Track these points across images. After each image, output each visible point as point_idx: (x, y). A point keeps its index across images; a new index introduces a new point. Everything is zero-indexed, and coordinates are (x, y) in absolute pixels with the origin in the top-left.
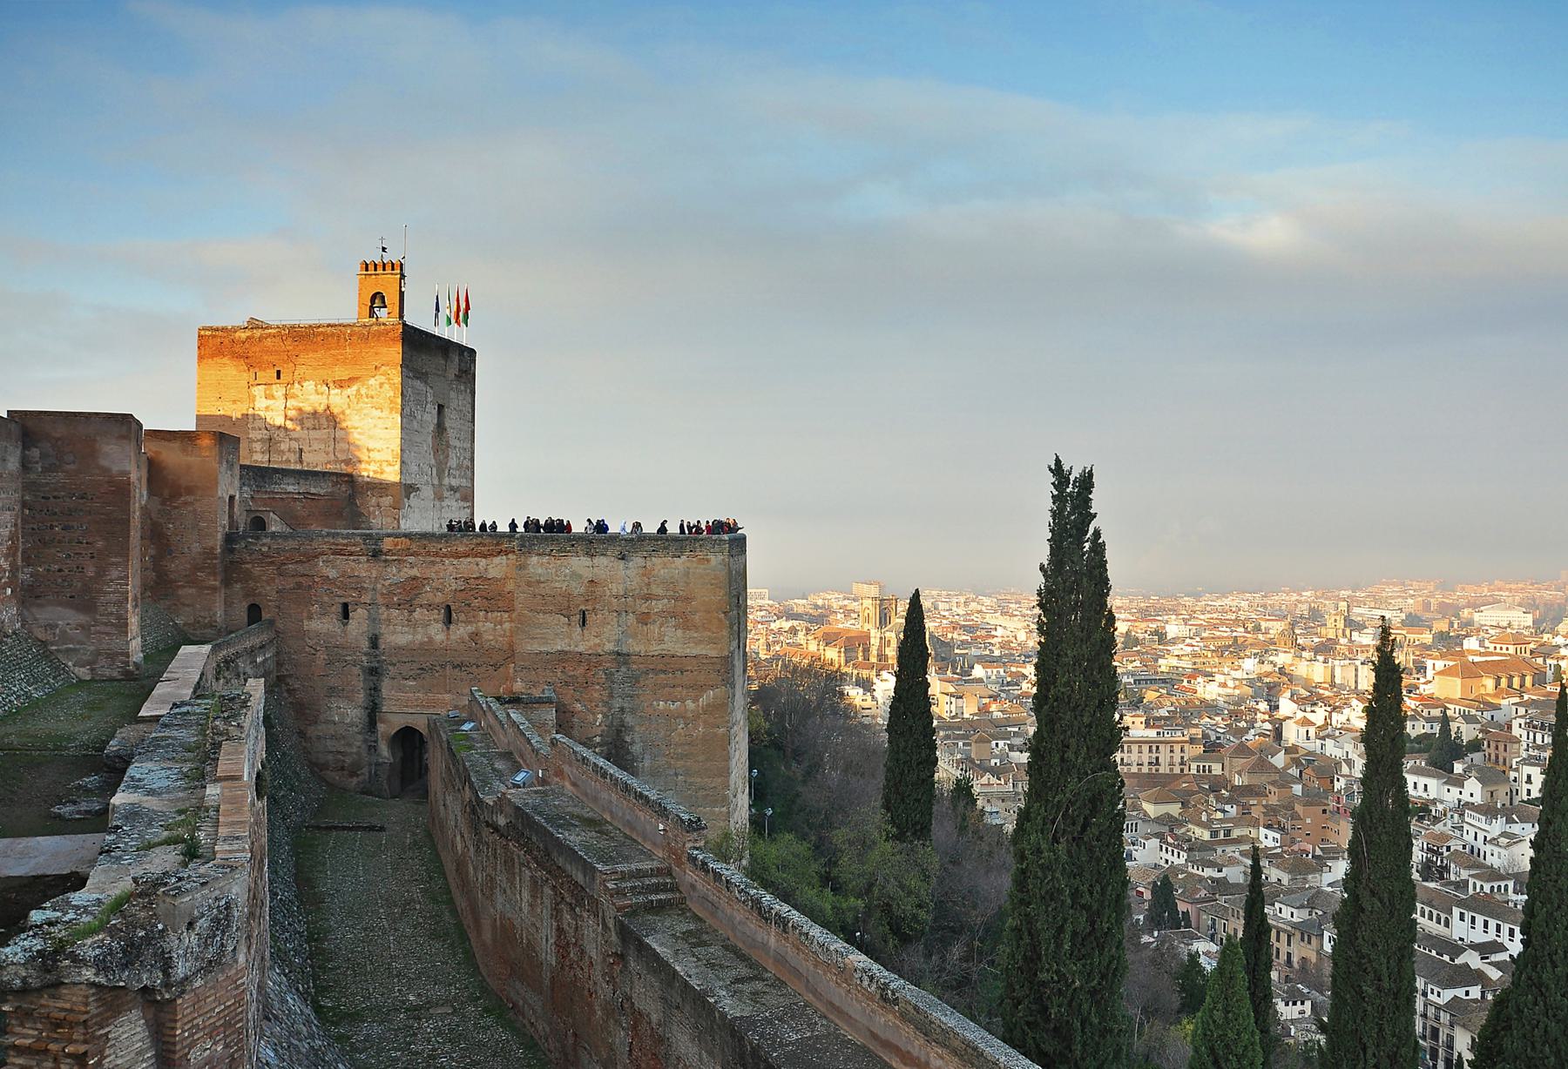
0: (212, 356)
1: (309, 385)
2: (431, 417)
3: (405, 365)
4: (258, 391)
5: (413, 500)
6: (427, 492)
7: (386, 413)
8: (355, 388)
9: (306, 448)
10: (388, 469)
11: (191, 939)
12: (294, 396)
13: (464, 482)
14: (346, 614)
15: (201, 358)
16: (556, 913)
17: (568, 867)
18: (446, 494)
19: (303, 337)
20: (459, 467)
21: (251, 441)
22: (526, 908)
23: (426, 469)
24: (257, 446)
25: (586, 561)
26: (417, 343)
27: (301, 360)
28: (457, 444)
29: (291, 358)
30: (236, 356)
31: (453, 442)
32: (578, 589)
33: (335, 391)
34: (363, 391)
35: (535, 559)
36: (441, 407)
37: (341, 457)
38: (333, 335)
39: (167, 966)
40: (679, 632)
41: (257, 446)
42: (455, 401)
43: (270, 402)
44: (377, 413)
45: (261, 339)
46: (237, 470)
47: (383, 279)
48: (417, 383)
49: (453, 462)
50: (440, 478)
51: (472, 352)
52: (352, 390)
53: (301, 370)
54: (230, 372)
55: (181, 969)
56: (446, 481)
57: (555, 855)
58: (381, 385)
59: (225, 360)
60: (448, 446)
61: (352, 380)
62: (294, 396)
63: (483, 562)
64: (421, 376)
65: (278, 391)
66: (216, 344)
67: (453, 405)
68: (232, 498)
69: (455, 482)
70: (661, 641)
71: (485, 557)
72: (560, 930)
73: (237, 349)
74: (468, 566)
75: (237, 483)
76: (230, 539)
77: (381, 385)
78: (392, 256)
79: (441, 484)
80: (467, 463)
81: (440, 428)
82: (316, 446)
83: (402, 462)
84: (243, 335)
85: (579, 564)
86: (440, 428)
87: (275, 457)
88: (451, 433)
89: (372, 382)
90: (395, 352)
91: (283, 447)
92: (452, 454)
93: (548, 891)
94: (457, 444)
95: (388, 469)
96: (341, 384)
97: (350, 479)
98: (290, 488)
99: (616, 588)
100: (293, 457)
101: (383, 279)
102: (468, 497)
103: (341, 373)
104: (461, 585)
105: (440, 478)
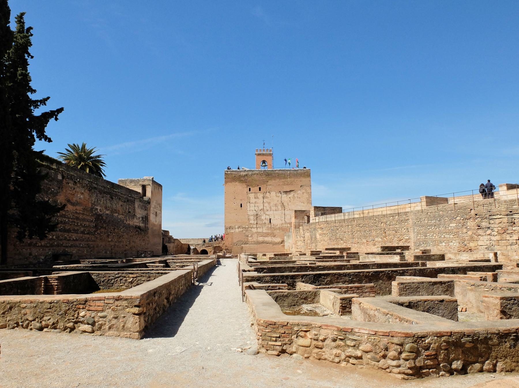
0: (231, 182)
1: (273, 194)
4: (252, 196)
7: (306, 204)
8: (292, 194)
12: (267, 198)
15: (226, 182)
21: (249, 216)
24: (252, 218)
27: (268, 183)
29: (265, 182)
30: (241, 181)
33: (285, 195)
34: (296, 195)
37: (288, 221)
38: (282, 174)
41: (252, 218)
43: (256, 200)
44: (302, 204)
45: (252, 175)
52: (291, 195)
54: (240, 188)
58: (303, 193)
61: (291, 191)
62: (267, 198)
65: (260, 195)
73: (242, 179)
77: (303, 193)
82: (277, 217)
89: (299, 192)
91: (263, 217)
96: (286, 192)
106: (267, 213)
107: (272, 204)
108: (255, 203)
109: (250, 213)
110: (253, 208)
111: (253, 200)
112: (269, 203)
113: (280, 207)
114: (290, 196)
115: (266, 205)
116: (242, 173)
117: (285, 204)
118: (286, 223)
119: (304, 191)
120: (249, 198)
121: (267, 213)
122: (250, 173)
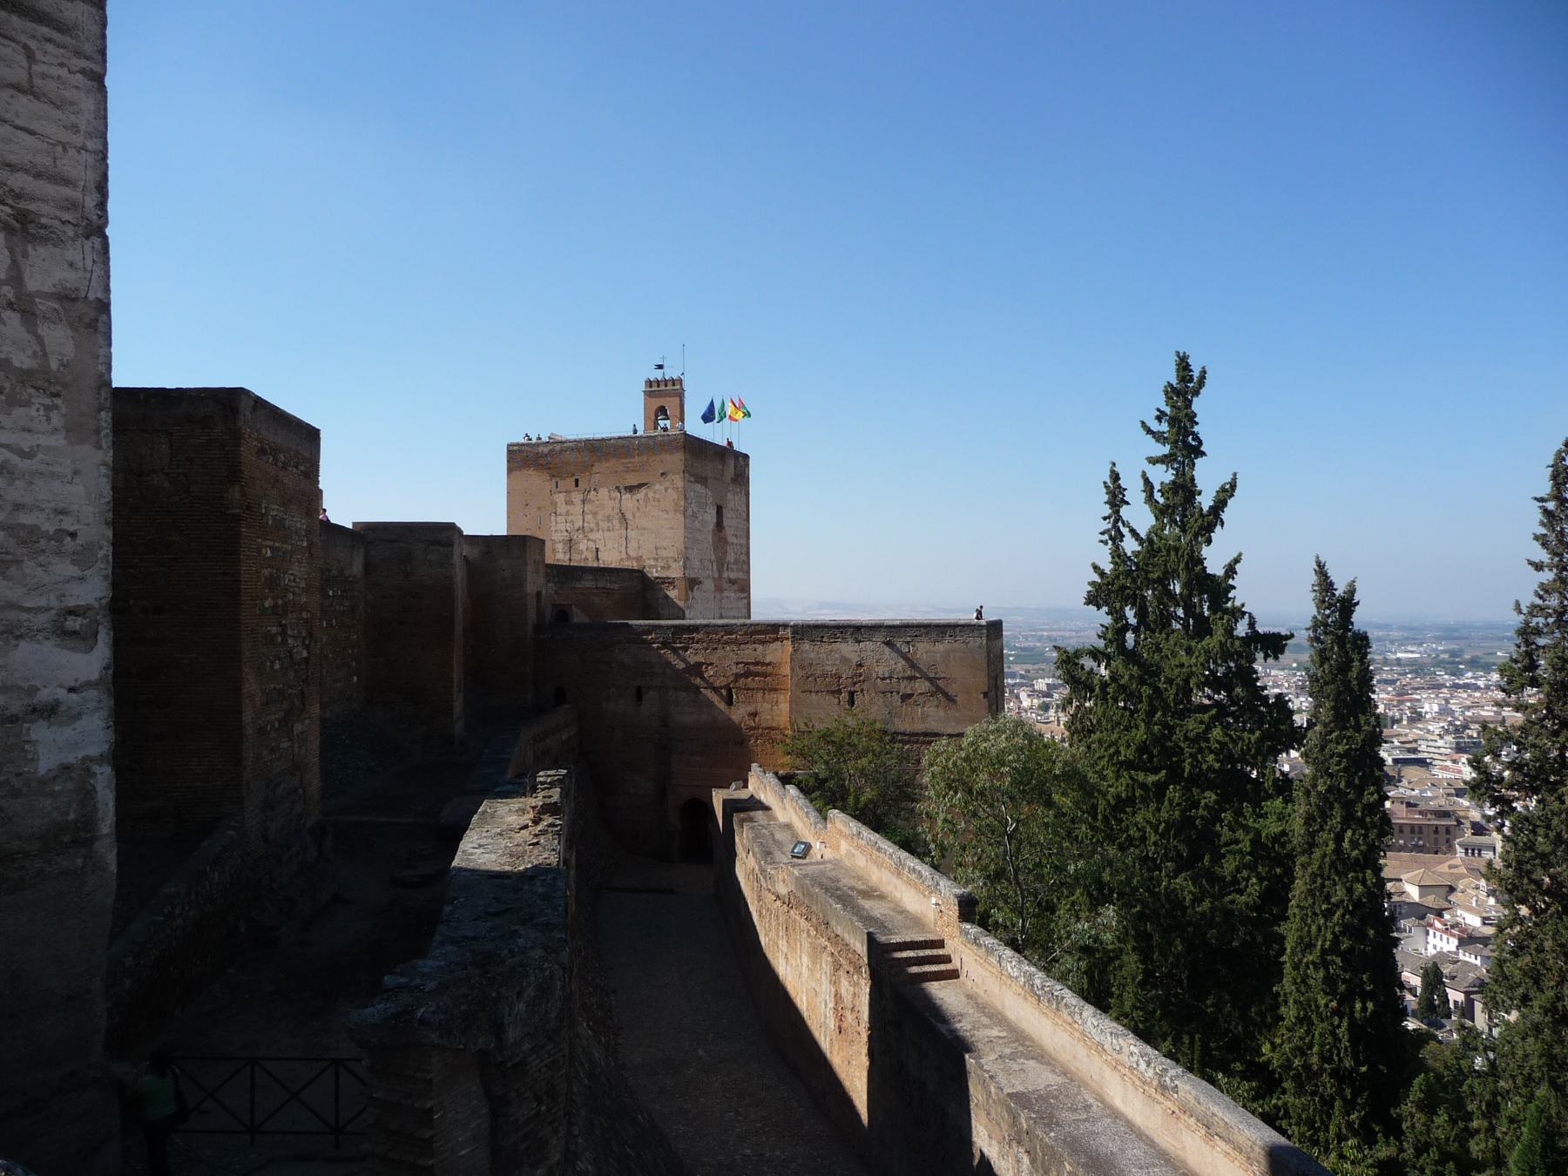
1: (603, 492)
2: (710, 517)
3: (687, 470)
4: (560, 498)
5: (697, 593)
6: (709, 585)
8: (643, 491)
9: (602, 549)
10: (674, 565)
11: (522, 1006)
12: (591, 501)
13: (741, 575)
14: (639, 695)
15: (510, 471)
16: (836, 983)
17: (846, 936)
18: (726, 586)
19: (597, 450)
20: (736, 562)
21: (554, 542)
22: (805, 972)
23: (707, 563)
24: (560, 547)
25: (856, 647)
26: (697, 449)
27: (595, 469)
28: (734, 540)
29: (588, 467)
31: (731, 539)
32: (846, 673)
33: (626, 496)
34: (651, 495)
35: (806, 646)
36: (719, 510)
37: (633, 554)
39: (498, 1029)
40: (941, 713)
41: (560, 547)
42: (732, 501)
46: (541, 570)
47: (664, 395)
48: (699, 488)
49: (731, 557)
50: (720, 573)
51: (746, 457)
53: (596, 478)
54: (536, 480)
55: (512, 1034)
56: (725, 575)
57: (833, 923)
59: (531, 472)
60: (726, 542)
61: (641, 486)
62: (591, 501)
63: (760, 648)
64: (702, 480)
65: (577, 497)
66: (524, 458)
67: (731, 505)
68: (539, 594)
69: (733, 576)
70: (924, 718)
71: (762, 642)
72: (838, 997)
73: (542, 461)
74: (750, 653)
75: (541, 580)
76: (539, 628)
78: (670, 373)
79: (720, 578)
80: (743, 558)
81: (719, 525)
83: (687, 559)
84: (546, 450)
85: (848, 649)
86: (719, 525)
87: (575, 557)
88: (729, 532)
89: (657, 487)
90: (677, 460)
91: (582, 547)
92: (730, 549)
93: (826, 958)
94: (734, 540)
95: (674, 565)
96: (631, 489)
97: (639, 576)
98: (588, 584)
99: (882, 670)
100: (591, 556)
101: (664, 395)
102: (744, 587)
103: (632, 480)
104: (740, 669)
105: (720, 573)
106: (591, 536)
107: (600, 517)
108: (567, 513)
109: (557, 537)
110: (562, 526)
111: (562, 508)
112: (595, 514)
113: (616, 522)
114: (639, 496)
115: (589, 517)
116: (540, 449)
117: (629, 516)
118: (629, 557)
119: (667, 484)
120: (554, 504)
121: (591, 536)
122: (558, 447)
